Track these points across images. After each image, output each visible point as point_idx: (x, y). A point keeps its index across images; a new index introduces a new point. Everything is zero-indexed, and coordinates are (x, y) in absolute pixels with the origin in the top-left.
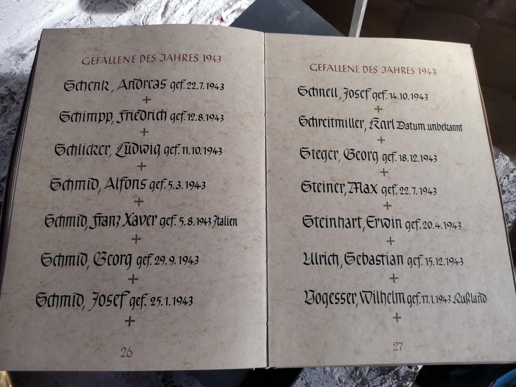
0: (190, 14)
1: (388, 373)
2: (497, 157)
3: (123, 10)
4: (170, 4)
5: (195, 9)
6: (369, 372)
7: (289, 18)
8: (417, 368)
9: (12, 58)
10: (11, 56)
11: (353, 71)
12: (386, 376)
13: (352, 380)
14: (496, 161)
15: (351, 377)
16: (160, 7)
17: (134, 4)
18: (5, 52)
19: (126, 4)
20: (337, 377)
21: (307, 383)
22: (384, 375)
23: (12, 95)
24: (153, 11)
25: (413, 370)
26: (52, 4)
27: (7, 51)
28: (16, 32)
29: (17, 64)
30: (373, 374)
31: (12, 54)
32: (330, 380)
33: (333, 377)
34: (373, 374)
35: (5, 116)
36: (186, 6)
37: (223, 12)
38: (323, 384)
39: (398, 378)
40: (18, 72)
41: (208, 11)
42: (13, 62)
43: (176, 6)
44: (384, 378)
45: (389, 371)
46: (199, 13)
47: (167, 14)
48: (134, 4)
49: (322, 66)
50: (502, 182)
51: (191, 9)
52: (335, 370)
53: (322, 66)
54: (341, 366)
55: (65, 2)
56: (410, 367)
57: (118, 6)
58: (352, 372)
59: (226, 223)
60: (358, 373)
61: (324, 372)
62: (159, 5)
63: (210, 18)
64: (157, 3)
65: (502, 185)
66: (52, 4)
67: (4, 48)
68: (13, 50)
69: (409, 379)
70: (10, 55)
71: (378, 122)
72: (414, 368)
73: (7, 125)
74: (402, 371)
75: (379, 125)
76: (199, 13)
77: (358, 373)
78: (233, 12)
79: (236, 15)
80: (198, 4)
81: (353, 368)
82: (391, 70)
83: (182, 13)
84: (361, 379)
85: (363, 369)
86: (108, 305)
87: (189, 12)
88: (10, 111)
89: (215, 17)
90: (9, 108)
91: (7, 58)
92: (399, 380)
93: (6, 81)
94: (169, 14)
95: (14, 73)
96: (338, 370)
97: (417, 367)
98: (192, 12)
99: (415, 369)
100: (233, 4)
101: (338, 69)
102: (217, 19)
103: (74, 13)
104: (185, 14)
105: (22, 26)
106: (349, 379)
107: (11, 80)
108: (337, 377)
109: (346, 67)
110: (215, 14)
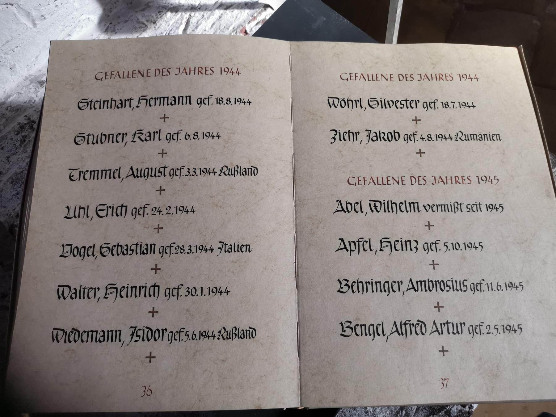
0: (212, 29)
1: (439, 413)
3: (143, 29)
4: (191, 20)
5: (217, 23)
6: (416, 412)
9: (31, 86)
10: (30, 84)
11: (387, 80)
16: (181, 23)
17: (155, 23)
18: (25, 80)
19: (146, 23)
23: (31, 123)
24: (174, 29)
26: (70, 28)
27: (26, 79)
28: (34, 59)
29: (36, 92)
31: (32, 82)
35: (25, 146)
36: (208, 21)
37: (247, 25)
40: (37, 99)
41: (232, 25)
42: (33, 90)
46: (222, 27)
47: (188, 30)
48: (155, 23)
51: (214, 24)
52: (378, 410)
54: (384, 406)
55: (84, 25)
56: (464, 406)
57: (137, 26)
59: (236, 250)
60: (404, 413)
61: (366, 412)
62: (180, 22)
63: (233, 31)
64: (178, 20)
66: (70, 28)
67: (23, 76)
68: (32, 77)
70: (29, 82)
71: (142, 134)
72: (467, 406)
73: (27, 155)
74: (455, 411)
75: (143, 137)
76: (222, 27)
77: (404, 413)
78: (257, 24)
79: (260, 26)
80: (220, 17)
81: (398, 408)
83: (204, 28)
85: (410, 408)
86: (136, 341)
87: (212, 26)
88: (29, 141)
89: (239, 30)
90: (28, 137)
91: (26, 86)
94: (191, 30)
95: (33, 101)
96: (381, 409)
97: (471, 405)
98: (214, 26)
99: (470, 408)
100: (257, 15)
101: (370, 78)
102: (241, 32)
103: (92, 35)
104: (207, 29)
105: (40, 52)
107: (30, 108)
109: (379, 76)
110: (239, 27)
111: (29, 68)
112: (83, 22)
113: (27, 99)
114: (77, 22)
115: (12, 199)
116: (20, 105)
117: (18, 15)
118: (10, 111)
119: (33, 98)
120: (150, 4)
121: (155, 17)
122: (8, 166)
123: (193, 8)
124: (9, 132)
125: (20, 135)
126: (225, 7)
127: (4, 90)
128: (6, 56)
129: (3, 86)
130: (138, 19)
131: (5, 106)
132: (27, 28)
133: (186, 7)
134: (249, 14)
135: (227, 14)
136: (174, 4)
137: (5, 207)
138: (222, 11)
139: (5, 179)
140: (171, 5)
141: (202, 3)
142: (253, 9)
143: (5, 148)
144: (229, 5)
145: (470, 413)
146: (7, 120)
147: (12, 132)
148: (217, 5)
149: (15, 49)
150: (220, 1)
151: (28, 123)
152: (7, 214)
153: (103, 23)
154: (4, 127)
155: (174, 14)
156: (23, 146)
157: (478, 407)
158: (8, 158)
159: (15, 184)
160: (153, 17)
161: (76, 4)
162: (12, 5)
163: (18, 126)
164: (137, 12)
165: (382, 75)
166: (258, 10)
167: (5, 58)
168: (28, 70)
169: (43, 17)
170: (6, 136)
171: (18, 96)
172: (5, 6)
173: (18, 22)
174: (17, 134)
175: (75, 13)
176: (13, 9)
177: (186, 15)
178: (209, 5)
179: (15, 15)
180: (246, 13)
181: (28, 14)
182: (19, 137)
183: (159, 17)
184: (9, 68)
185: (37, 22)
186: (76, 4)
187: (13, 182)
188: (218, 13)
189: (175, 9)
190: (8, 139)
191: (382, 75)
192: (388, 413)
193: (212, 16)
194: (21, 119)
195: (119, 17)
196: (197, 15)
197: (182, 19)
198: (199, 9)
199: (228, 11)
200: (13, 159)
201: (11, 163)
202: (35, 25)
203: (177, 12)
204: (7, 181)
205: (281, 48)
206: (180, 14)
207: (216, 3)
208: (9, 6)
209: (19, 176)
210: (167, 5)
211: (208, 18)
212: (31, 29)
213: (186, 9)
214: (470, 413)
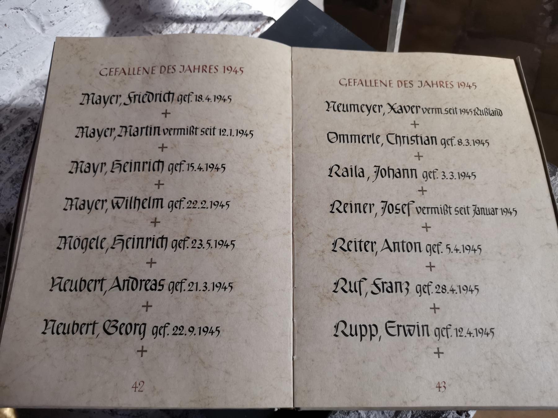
2: (554, 174)
7: (315, 34)
9: (37, 90)
10: (36, 88)
11: (386, 86)
14: (551, 179)
18: (31, 84)
19: (152, 33)
27: (32, 83)
28: (41, 64)
31: (37, 86)
49: (352, 81)
53: (352, 81)
64: (183, 30)
67: (29, 80)
68: (38, 81)
70: (35, 86)
80: (225, 28)
81: (393, 413)
82: (428, 84)
85: (404, 415)
91: (32, 90)
93: (29, 112)
95: (38, 104)
97: (468, 413)
101: (368, 84)
109: (378, 82)
111: (36, 72)
112: (91, 21)
113: (32, 102)
115: (11, 198)
117: (27, 20)
118: (14, 113)
119: (38, 101)
120: (157, 15)
121: (161, 27)
122: (8, 166)
123: (198, 20)
124: (12, 133)
126: (230, 19)
127: (10, 93)
128: (13, 60)
130: (145, 29)
131: (9, 108)
132: (36, 33)
133: (191, 19)
134: (253, 26)
135: (232, 26)
136: (181, 16)
137: (3, 206)
138: (226, 23)
139: (5, 178)
140: (178, 16)
142: (257, 21)
143: (7, 148)
146: (11, 122)
148: (222, 17)
149: (23, 53)
150: (225, 14)
151: (32, 125)
152: (5, 213)
153: (110, 32)
154: (8, 128)
155: (180, 25)
156: (25, 146)
158: (9, 158)
159: (15, 184)
160: (159, 27)
161: (85, 13)
162: (22, 10)
163: (21, 128)
164: (143, 22)
165: (381, 81)
166: (262, 22)
167: (12, 62)
168: (35, 74)
169: (52, 23)
172: (15, 11)
174: (20, 136)
175: (83, 21)
176: (23, 14)
177: (192, 26)
178: (215, 17)
180: (250, 25)
181: (37, 20)
182: (22, 138)
184: (15, 72)
185: (46, 27)
186: (85, 13)
187: (13, 181)
188: (223, 24)
189: (181, 20)
190: (11, 140)
191: (381, 81)
193: (216, 28)
194: (25, 121)
195: (126, 27)
196: (201, 28)
197: (187, 29)
198: (205, 20)
199: (233, 23)
201: (12, 163)
202: (43, 30)
204: (7, 181)
207: (222, 15)
208: (19, 10)
209: (19, 176)
210: (173, 16)
212: (40, 34)
213: (192, 21)
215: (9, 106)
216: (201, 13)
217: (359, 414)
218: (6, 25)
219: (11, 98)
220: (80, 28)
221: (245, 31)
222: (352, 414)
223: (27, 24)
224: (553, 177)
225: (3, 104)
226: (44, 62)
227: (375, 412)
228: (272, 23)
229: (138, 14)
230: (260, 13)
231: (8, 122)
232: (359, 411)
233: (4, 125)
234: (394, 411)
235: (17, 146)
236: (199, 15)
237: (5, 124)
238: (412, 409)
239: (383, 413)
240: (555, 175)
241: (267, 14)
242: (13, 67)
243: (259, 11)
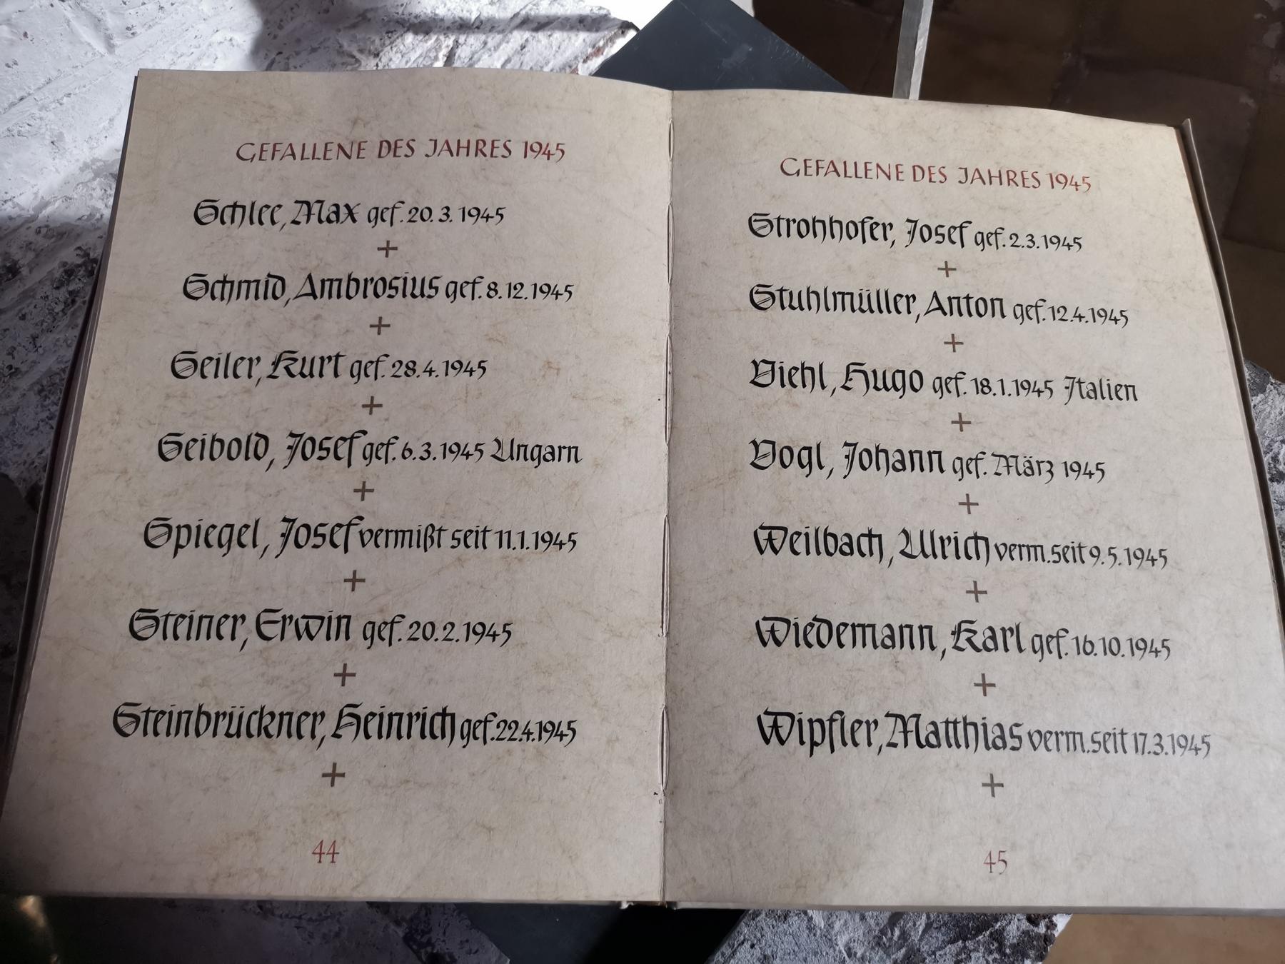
4: (459, 51)
5: (516, 60)
6: (924, 931)
8: (1051, 926)
10: (94, 179)
12: (969, 944)
13: (881, 953)
14: (1254, 401)
15: (878, 944)
16: (436, 58)
17: (377, 55)
18: (82, 170)
19: (358, 56)
20: (841, 942)
21: (765, 957)
22: (964, 941)
25: (1042, 929)
27: (86, 166)
28: (106, 124)
30: (937, 937)
31: (97, 175)
32: (825, 949)
33: (831, 943)
34: (937, 937)
35: (73, 314)
36: (496, 55)
38: (805, 960)
39: (1000, 950)
41: (547, 64)
42: (98, 193)
43: (473, 54)
44: (965, 947)
45: (979, 931)
48: (377, 55)
50: (1275, 450)
52: (837, 926)
55: (219, 56)
56: (1033, 919)
57: (338, 60)
58: (881, 931)
60: (897, 933)
61: (810, 929)
62: (432, 55)
64: (429, 50)
65: (1275, 459)
68: (99, 164)
69: (1032, 953)
70: (91, 175)
72: (1043, 924)
74: (1014, 930)
77: (897, 933)
80: (523, 47)
81: (884, 918)
84: (903, 951)
85: (910, 924)
91: (85, 184)
92: (1005, 955)
93: (78, 235)
95: (98, 216)
97: (1051, 921)
99: (1048, 928)
106: (873, 948)
108: (841, 942)
113: (85, 212)
114: (204, 47)
116: (68, 224)
117: (74, 23)
118: (45, 236)
119: (99, 210)
120: (369, 15)
121: (377, 42)
123: (463, 26)
125: (63, 290)
126: (535, 25)
127: (35, 189)
128: (43, 114)
129: (33, 182)
131: (34, 226)
132: (94, 54)
133: (447, 24)
134: (588, 41)
135: (539, 41)
136: (423, 17)
137: (20, 446)
138: (527, 35)
139: (23, 383)
140: (416, 17)
141: (485, 15)
142: (597, 31)
143: (28, 317)
144: (543, 21)
145: (1047, 939)
146: (37, 256)
147: (48, 283)
148: (518, 21)
150: (523, 12)
151: (84, 264)
155: (420, 37)
156: (69, 313)
157: (1069, 925)
158: (34, 338)
159: (46, 397)
161: (205, 8)
166: (608, 34)
167: (41, 119)
168: (91, 149)
169: (130, 31)
170: (32, 289)
171: (65, 204)
173: (74, 39)
174: (57, 288)
175: (202, 26)
178: (500, 21)
179: (68, 22)
180: (579, 41)
181: (97, 23)
182: (62, 294)
183: (387, 42)
184: (48, 142)
185: (117, 41)
186: (205, 8)
188: (518, 37)
189: (424, 27)
192: (861, 932)
193: (504, 45)
194: (69, 255)
195: (298, 41)
196: (471, 43)
197: (437, 48)
198: (478, 28)
199: (541, 35)
200: (46, 341)
201: (40, 350)
202: (111, 47)
203: (427, 33)
205: (651, 104)
206: (434, 38)
207: (516, 15)
210: (406, 17)
211: (496, 48)
213: (448, 28)
214: (1047, 939)
215: (33, 219)
216: (470, 12)
217: (810, 919)
218: (25, 35)
219: (36, 203)
220: (194, 42)
221: (568, 54)
222: (794, 920)
223: (72, 32)
224: (1261, 396)
225: (19, 216)
226: (111, 120)
227: (846, 915)
228: (631, 34)
229: (327, 11)
230: (604, 12)
231: (31, 255)
232: (810, 912)
233: (21, 262)
234: (887, 914)
235: (51, 311)
236: (465, 15)
237: (24, 259)
238: (928, 911)
239: (863, 918)
240: (1263, 391)
241: (620, 14)
242: (43, 131)
243: (600, 8)
